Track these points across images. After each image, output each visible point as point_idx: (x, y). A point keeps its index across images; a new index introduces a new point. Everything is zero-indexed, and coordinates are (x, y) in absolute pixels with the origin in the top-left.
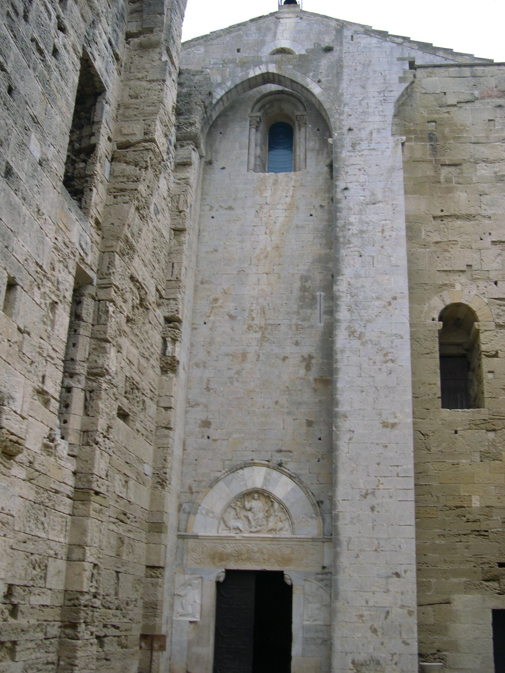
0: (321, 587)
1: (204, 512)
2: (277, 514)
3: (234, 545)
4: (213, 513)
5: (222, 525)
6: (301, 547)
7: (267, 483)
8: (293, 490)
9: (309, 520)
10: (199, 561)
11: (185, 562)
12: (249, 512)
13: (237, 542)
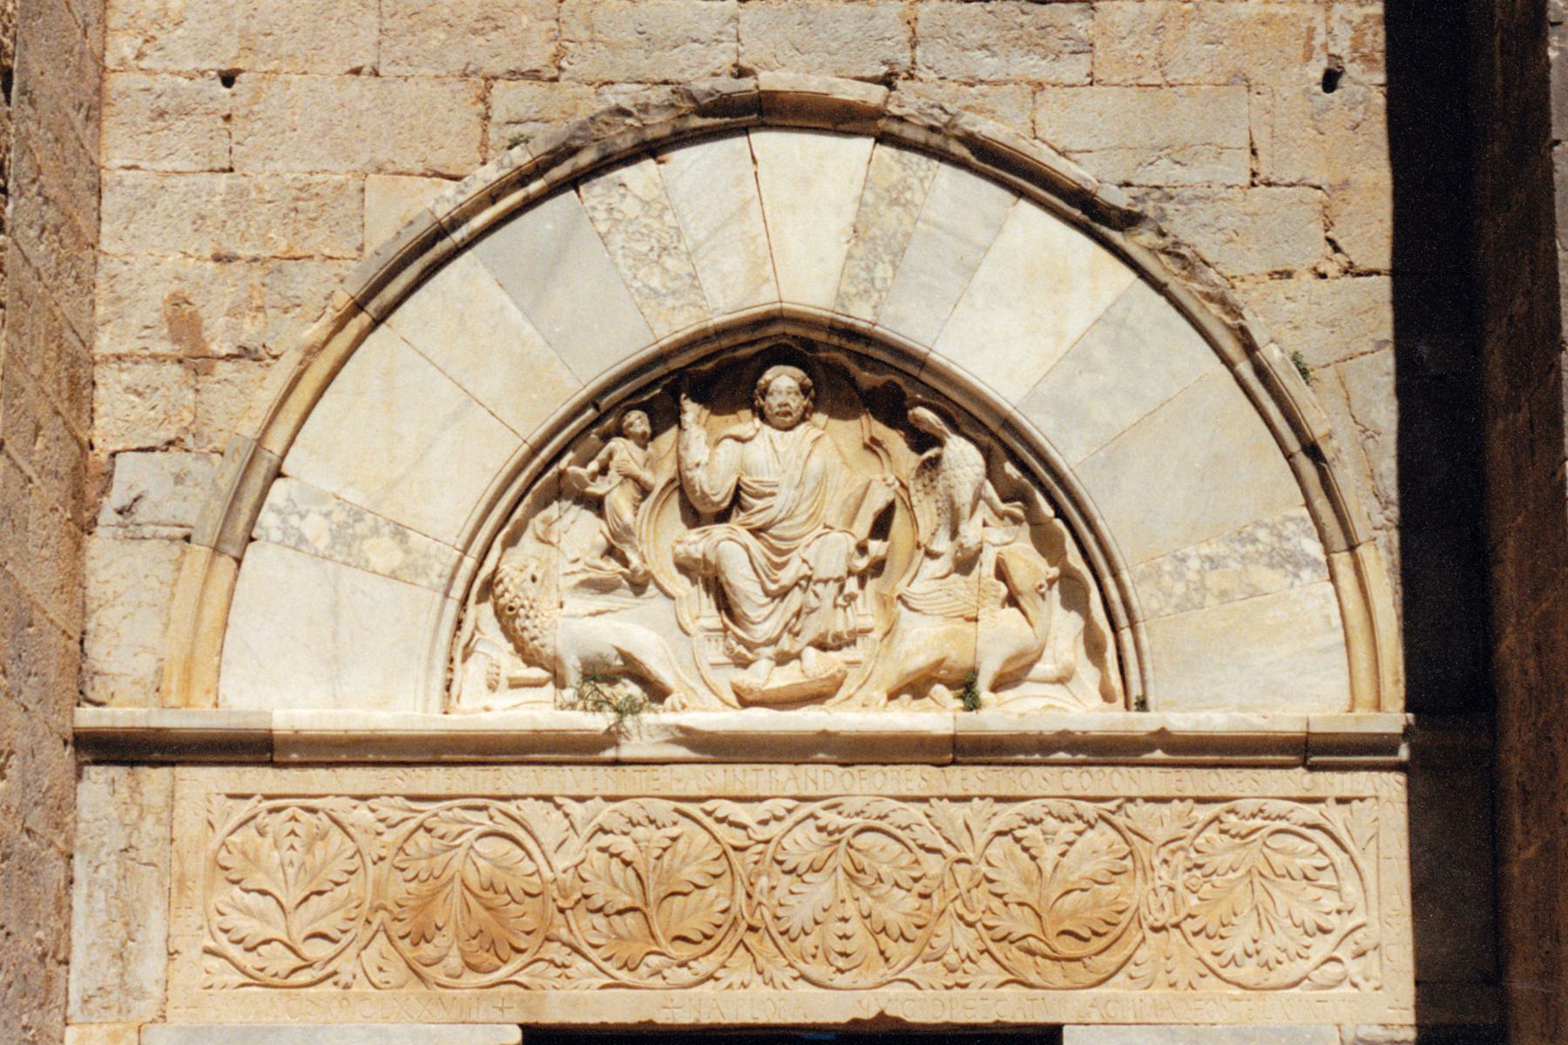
1: (315, 527)
3: (606, 813)
4: (400, 532)
5: (495, 649)
6: (1203, 813)
7: (883, 271)
8: (1109, 322)
11: (149, 969)
12: (719, 530)
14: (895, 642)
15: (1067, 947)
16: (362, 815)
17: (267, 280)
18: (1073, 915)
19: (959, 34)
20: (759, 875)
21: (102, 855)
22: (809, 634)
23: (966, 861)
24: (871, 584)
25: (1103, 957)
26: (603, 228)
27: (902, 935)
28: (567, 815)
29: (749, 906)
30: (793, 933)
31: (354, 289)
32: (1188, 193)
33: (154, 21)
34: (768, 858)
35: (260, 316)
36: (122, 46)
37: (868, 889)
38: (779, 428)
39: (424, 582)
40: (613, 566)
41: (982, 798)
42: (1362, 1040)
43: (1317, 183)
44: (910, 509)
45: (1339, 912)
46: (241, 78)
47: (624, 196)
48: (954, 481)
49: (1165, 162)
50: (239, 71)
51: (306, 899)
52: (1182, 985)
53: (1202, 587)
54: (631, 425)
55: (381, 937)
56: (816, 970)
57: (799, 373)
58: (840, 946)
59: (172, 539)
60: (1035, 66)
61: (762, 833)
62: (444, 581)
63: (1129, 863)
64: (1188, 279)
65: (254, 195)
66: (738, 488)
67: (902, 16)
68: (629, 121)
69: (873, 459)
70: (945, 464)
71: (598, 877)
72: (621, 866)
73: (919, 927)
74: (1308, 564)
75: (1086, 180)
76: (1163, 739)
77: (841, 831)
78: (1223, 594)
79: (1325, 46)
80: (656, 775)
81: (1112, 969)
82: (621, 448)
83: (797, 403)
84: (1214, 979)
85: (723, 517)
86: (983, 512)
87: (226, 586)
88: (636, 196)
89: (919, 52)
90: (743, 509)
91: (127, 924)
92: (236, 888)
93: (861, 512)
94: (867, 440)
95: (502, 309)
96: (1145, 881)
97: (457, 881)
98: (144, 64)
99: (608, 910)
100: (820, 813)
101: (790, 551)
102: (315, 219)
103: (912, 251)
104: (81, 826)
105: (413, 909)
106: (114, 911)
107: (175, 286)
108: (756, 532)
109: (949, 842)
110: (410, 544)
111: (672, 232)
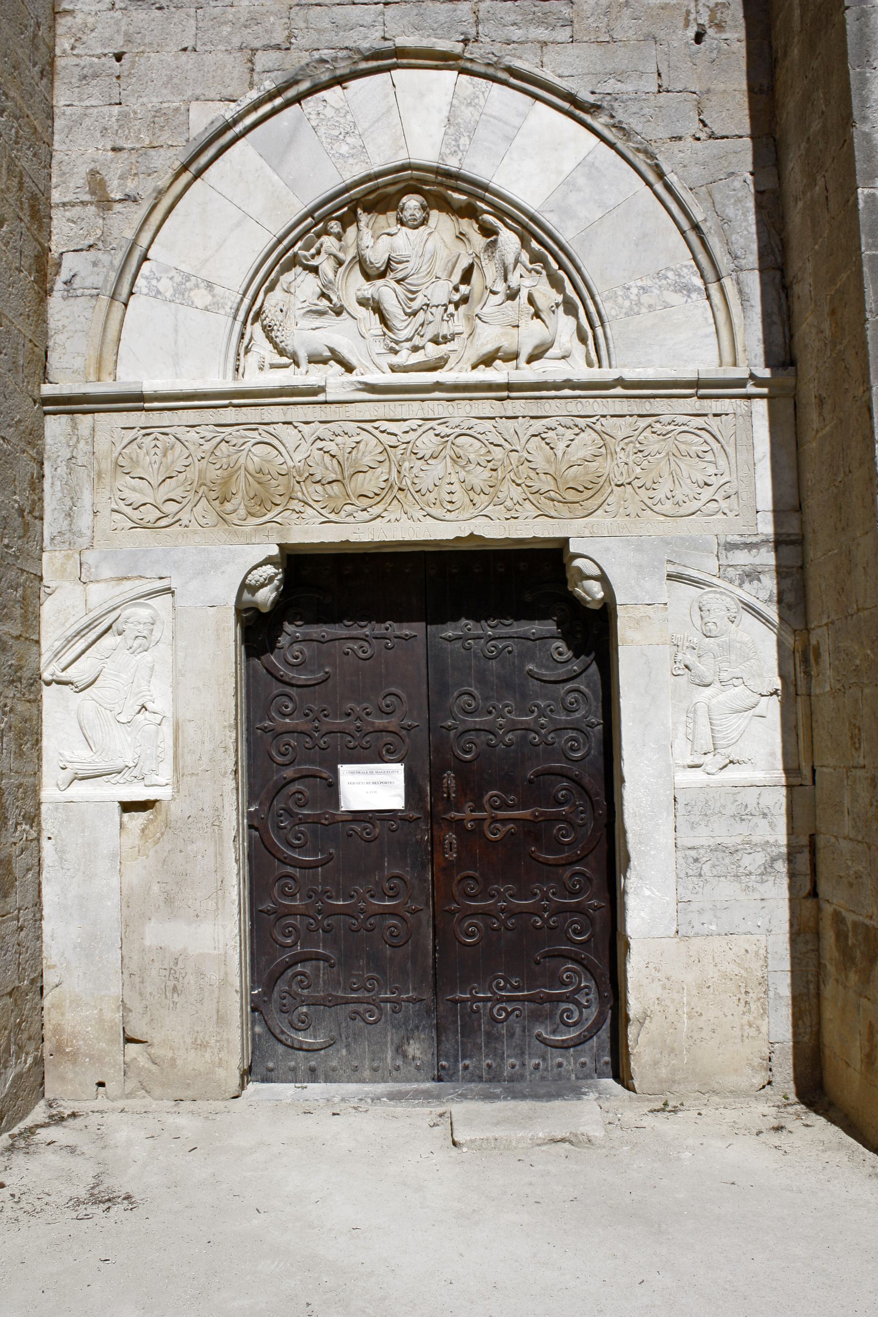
0: (749, 608)
1: (165, 286)
2: (514, 280)
3: (321, 431)
4: (210, 286)
5: (262, 349)
6: (643, 423)
7: (465, 141)
9: (676, 299)
10: (151, 514)
11: (84, 521)
12: (380, 282)
13: (330, 412)
14: (475, 340)
15: (571, 496)
16: (192, 435)
17: (140, 160)
18: (575, 478)
19: (502, 18)
20: (404, 461)
21: (58, 462)
22: (429, 336)
23: (517, 451)
24: (462, 308)
25: (590, 501)
26: (314, 124)
27: (482, 490)
28: (300, 431)
29: (398, 478)
30: (423, 492)
31: (183, 158)
32: (625, 97)
33: (80, 30)
34: (409, 451)
35: (136, 178)
36: (63, 44)
37: (463, 467)
38: (410, 228)
39: (222, 311)
40: (325, 302)
41: (524, 417)
42: (729, 543)
43: (693, 90)
44: (481, 269)
45: (716, 475)
46: (126, 56)
47: (325, 106)
48: (504, 252)
49: (612, 81)
50: (124, 53)
51: (164, 480)
52: (633, 515)
53: (639, 303)
54: (332, 228)
55: (204, 500)
56: (437, 511)
57: (420, 198)
58: (448, 498)
59: (92, 296)
60: (542, 33)
61: (406, 437)
62: (233, 311)
63: (605, 449)
64: (627, 141)
65: (132, 115)
66: (389, 259)
67: (472, 9)
68: (327, 66)
69: (461, 244)
70: (500, 244)
71: (318, 464)
72: (330, 458)
73: (491, 487)
74: (695, 290)
75: (572, 88)
76: (620, 382)
77: (448, 436)
78: (650, 306)
79: (696, 19)
80: (347, 409)
81: (596, 508)
82: (329, 242)
83: (419, 214)
84: (649, 512)
85: (382, 275)
86: (520, 269)
87: (119, 317)
88: (331, 106)
89: (480, 27)
90: (392, 271)
91: (72, 498)
92: (127, 477)
93: (455, 271)
94: (458, 234)
95: (262, 168)
96: (612, 460)
97: (243, 468)
98: (75, 52)
99: (324, 482)
100: (436, 427)
101: (417, 292)
102: (164, 127)
103: (481, 132)
104: (47, 447)
105: (220, 484)
106: (65, 491)
107: (92, 166)
108: (398, 282)
109: (506, 440)
110: (216, 292)
111: (351, 124)
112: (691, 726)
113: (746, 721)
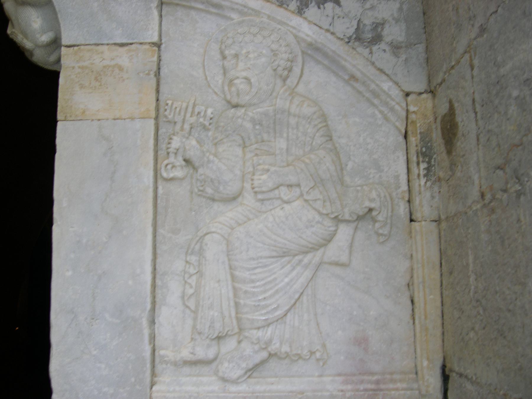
112: (193, 281)
113: (308, 274)
